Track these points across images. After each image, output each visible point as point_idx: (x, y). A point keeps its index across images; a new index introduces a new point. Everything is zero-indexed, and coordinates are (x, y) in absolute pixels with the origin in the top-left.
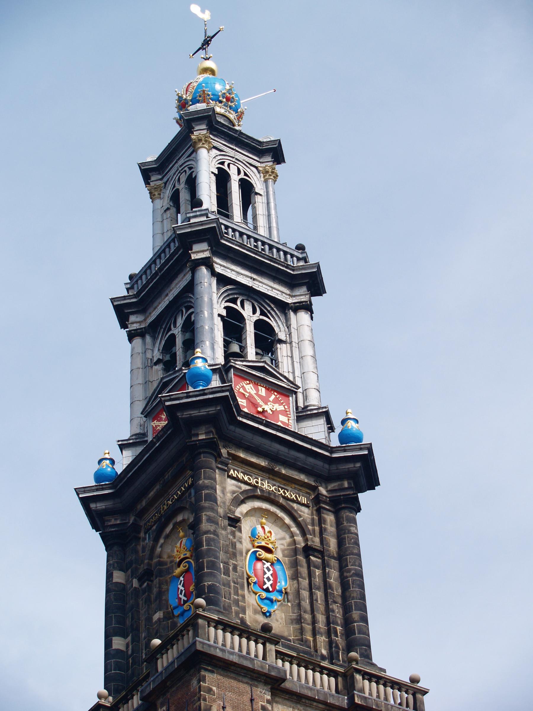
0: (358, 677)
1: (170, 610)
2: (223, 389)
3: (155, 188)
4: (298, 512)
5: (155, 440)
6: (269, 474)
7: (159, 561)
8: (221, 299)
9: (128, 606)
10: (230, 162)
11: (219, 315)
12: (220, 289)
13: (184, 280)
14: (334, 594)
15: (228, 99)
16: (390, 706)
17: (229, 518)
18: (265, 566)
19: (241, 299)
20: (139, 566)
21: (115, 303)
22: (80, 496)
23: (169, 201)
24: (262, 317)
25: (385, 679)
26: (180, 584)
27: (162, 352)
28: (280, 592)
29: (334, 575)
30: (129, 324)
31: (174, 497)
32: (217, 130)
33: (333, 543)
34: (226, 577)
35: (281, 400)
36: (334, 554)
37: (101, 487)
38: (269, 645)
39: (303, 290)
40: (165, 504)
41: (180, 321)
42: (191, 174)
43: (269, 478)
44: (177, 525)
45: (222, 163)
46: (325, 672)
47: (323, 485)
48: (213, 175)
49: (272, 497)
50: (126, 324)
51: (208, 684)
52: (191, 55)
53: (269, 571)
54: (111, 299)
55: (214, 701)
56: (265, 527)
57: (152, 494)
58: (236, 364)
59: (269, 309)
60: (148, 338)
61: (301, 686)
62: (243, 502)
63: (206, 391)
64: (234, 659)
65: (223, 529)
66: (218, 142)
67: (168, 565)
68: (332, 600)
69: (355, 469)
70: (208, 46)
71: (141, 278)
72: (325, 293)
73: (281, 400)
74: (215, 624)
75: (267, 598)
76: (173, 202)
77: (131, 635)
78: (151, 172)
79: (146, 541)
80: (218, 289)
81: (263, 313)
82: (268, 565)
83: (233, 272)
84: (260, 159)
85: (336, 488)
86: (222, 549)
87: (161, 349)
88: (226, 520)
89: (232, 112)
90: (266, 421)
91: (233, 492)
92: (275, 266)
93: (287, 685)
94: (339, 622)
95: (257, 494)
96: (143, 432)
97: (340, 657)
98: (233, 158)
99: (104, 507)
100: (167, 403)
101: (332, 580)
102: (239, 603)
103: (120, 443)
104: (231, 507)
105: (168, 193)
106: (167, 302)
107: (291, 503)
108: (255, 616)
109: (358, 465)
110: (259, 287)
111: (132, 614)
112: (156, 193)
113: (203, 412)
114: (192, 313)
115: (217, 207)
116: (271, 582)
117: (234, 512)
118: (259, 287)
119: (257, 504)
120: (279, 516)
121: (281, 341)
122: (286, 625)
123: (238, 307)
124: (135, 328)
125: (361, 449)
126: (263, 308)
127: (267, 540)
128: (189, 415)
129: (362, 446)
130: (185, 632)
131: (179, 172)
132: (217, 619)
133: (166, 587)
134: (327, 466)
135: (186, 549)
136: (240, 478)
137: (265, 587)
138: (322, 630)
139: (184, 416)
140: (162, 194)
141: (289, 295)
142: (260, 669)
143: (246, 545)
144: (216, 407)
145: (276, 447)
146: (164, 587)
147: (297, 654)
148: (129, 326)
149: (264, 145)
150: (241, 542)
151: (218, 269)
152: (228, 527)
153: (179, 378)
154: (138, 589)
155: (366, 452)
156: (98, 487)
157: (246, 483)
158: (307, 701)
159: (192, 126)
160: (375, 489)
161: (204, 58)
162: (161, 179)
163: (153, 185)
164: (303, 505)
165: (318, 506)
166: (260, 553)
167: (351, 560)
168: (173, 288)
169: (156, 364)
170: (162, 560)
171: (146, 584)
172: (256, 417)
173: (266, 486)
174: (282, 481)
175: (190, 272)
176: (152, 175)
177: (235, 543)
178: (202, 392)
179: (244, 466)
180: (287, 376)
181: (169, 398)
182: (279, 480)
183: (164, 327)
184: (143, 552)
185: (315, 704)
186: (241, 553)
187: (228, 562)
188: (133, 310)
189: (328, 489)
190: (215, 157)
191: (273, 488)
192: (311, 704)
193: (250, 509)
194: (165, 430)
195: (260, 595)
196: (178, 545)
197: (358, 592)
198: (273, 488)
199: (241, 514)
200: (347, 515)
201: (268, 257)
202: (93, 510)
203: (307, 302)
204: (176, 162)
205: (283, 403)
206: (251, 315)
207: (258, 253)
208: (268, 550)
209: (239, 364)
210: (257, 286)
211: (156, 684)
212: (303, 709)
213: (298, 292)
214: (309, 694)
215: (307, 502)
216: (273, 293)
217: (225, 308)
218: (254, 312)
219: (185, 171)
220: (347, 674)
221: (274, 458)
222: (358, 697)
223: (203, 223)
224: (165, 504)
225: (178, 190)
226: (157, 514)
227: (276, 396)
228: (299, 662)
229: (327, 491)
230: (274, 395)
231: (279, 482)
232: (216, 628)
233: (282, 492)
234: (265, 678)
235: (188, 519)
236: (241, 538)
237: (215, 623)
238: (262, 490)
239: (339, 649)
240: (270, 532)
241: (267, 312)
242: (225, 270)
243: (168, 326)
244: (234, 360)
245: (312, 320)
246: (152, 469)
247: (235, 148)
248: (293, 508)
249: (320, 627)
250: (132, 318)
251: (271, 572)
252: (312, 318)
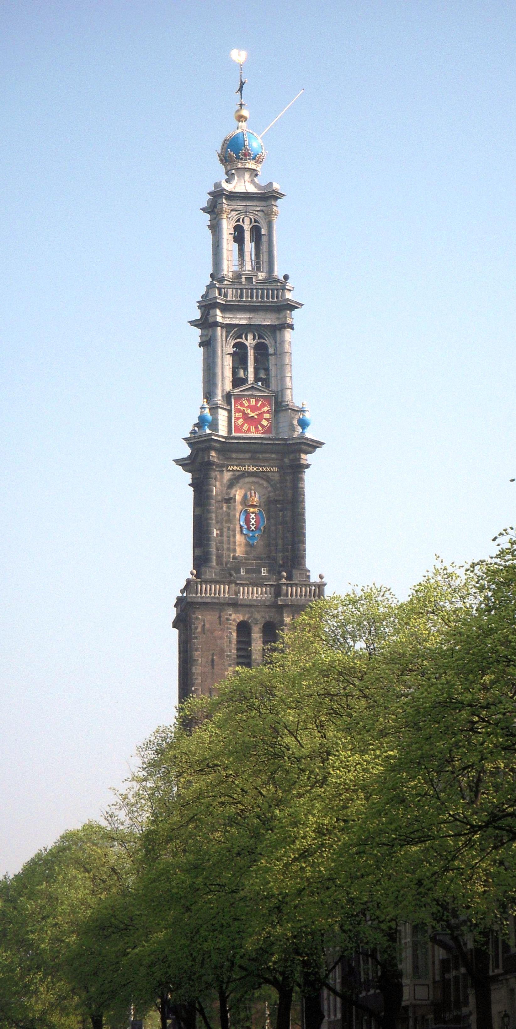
11: (228, 354)
24: (259, 341)
29: (289, 513)
33: (290, 492)
81: (260, 337)
82: (253, 516)
119: (247, 480)
121: (271, 355)
123: (243, 340)
173: (251, 469)
191: (255, 469)
198: (255, 469)
209: (237, 391)
218: (254, 339)
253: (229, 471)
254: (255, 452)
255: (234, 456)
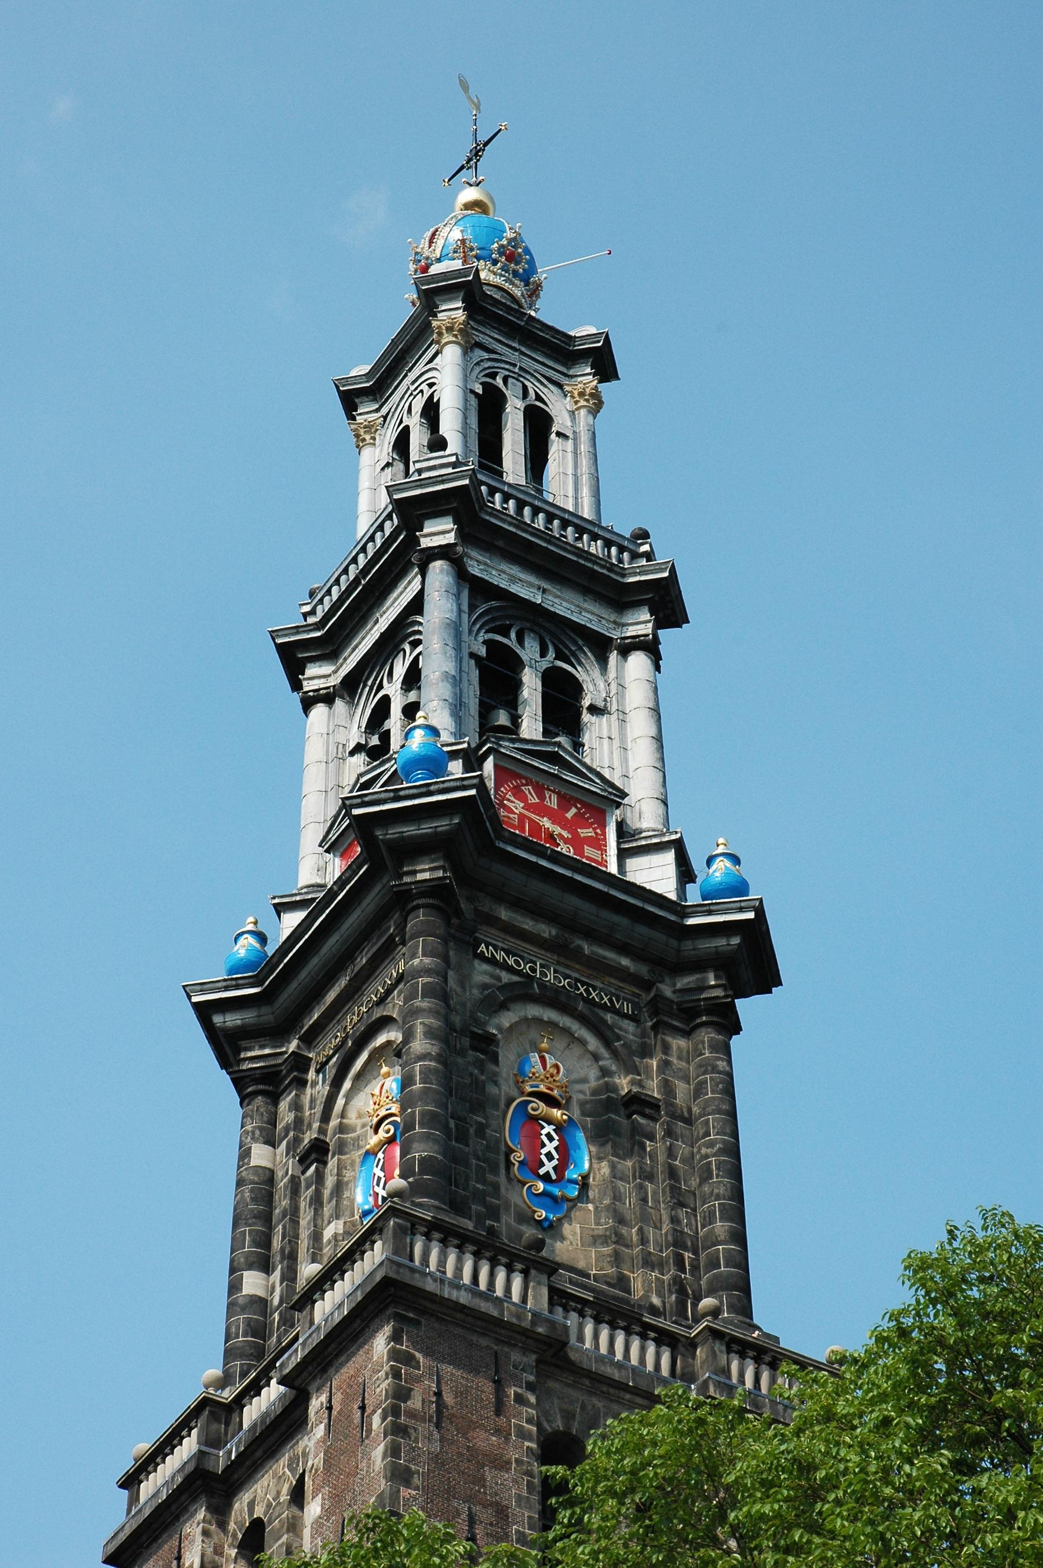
0: (719, 1347)
1: (357, 1217)
2: (465, 783)
3: (365, 427)
4: (614, 1031)
5: (335, 888)
6: (559, 955)
7: (341, 1123)
8: (478, 626)
9: (277, 1211)
10: (507, 373)
11: (472, 655)
12: (477, 607)
13: (408, 590)
14: (680, 1188)
15: (511, 258)
16: (780, 1407)
17: (472, 1032)
18: (544, 1132)
19: (518, 627)
20: (301, 1136)
21: (279, 641)
22: (195, 999)
23: (390, 450)
25: (772, 1354)
26: (377, 1166)
27: (365, 732)
28: (574, 1182)
30: (304, 679)
31: (371, 998)
32: (483, 311)
34: (462, 1146)
35: (588, 818)
36: (683, 1113)
37: (234, 983)
38: (538, 1274)
39: (644, 615)
40: (354, 1014)
41: (400, 669)
42: (432, 396)
43: (559, 963)
44: (377, 1055)
45: (493, 376)
46: (652, 1335)
47: (667, 980)
48: (473, 396)
49: (563, 998)
50: (300, 679)
51: (407, 1346)
52: (446, 180)
53: (551, 1142)
54: (271, 632)
55: (418, 1380)
56: (547, 1056)
57: (331, 996)
58: (501, 746)
59: (573, 648)
60: (339, 704)
61: (600, 1359)
62: (504, 1006)
63: (432, 788)
64: (464, 1298)
65: (459, 1054)
66: (488, 336)
67: (358, 1132)
68: (676, 1201)
69: (729, 948)
70: (478, 160)
71: (329, 592)
72: (688, 622)
73: (588, 818)
74: (426, 1230)
75: (545, 1194)
76: (398, 454)
77: (280, 1267)
78: (358, 397)
79: (317, 1087)
80: (472, 608)
82: (548, 1129)
83: (503, 576)
84: (569, 368)
85: (692, 986)
86: (456, 1092)
87: (364, 725)
88: (466, 1036)
89: (517, 282)
90: (553, 850)
91: (485, 987)
92: (587, 567)
93: (573, 1356)
94: (689, 1244)
95: (531, 991)
96: (323, 882)
97: (688, 1312)
98: (515, 365)
99: (239, 1022)
100: (356, 812)
101: (677, 1163)
102: (485, 1199)
103: (276, 901)
104: (479, 1014)
105: (390, 435)
106: (377, 636)
107: (601, 1013)
108: (521, 1227)
109: (736, 941)
110: (555, 605)
111: (284, 1227)
112: (367, 437)
113: (426, 828)
114: (420, 653)
115: (479, 457)
116: (555, 1162)
117: (485, 1024)
118: (555, 605)
119: (534, 1011)
120: (575, 1037)
121: (593, 709)
122: (582, 1246)
123: (511, 641)
124: (316, 687)
125: (741, 910)
126: (561, 647)
127: (550, 1082)
128: (397, 835)
129: (743, 904)
130: (367, 1246)
131: (411, 394)
132: (430, 1219)
133: (353, 1173)
134: (674, 943)
135: (390, 1098)
136: (498, 958)
137: (542, 1171)
138: (653, 1258)
139: (388, 836)
140: (377, 437)
141: (615, 622)
142: (514, 1320)
143: (507, 1089)
144: (451, 820)
145: (573, 901)
146: (348, 1175)
147: (594, 1297)
148: (305, 683)
149: (576, 343)
150: (496, 1083)
151: (475, 570)
152: (470, 1052)
153: (390, 773)
154: (297, 1179)
155: (751, 915)
156: (229, 983)
157: (510, 969)
158: (612, 1391)
159: (435, 303)
160: (771, 993)
161: (468, 183)
162: (377, 410)
163: (362, 421)
164: (626, 1016)
165: (655, 1020)
166: (534, 1105)
167: (715, 1124)
168: (388, 609)
169: (352, 753)
170: (344, 1121)
171: (313, 1168)
172: (532, 841)
173: (550, 977)
174: (586, 970)
175: (419, 576)
176: (361, 403)
177: (484, 1083)
178: (424, 790)
179: (507, 937)
180: (607, 776)
181: (359, 801)
182: (577, 966)
183: (370, 683)
184: (311, 1108)
185: (628, 1396)
186: (496, 1105)
187: (465, 1119)
188: (313, 654)
189: (677, 988)
190: (478, 364)
191: (564, 983)
192: (619, 1397)
193: (517, 1019)
194: (354, 867)
195: (531, 1186)
196: (377, 1092)
197: (729, 1185)
198: (564, 983)
199: (500, 1029)
200: (712, 1038)
201: (573, 549)
202: (218, 1027)
203: (648, 635)
204: (406, 375)
205: (592, 823)
206: (538, 659)
207: (552, 540)
208: (551, 1101)
209: (507, 747)
210: (551, 603)
211: (307, 1351)
212: (604, 1407)
213: (630, 617)
214: (617, 1375)
215: (632, 1012)
216: (582, 618)
217: (485, 642)
218: (543, 654)
219: (422, 391)
220: (696, 1340)
221: (569, 924)
222: (715, 1386)
223: (444, 478)
224: (354, 1014)
225: (407, 428)
226: (339, 1034)
227: (579, 809)
228: (598, 1314)
229: (674, 992)
230: (576, 807)
231: (577, 971)
232: (428, 1236)
233: (582, 990)
234: (524, 1339)
235: (396, 1039)
236: (496, 1074)
237: (426, 1227)
238: (542, 985)
239: (687, 1296)
240: (557, 1067)
241: (569, 654)
242: (487, 571)
243: (378, 682)
244: (496, 738)
245: (660, 672)
246: (332, 943)
247: (516, 345)
248: (605, 1022)
249: (650, 1253)
250: (311, 670)
251: (556, 1143)
252: (658, 668)
253: (482, 957)
254: (569, 924)
255: (504, 914)
